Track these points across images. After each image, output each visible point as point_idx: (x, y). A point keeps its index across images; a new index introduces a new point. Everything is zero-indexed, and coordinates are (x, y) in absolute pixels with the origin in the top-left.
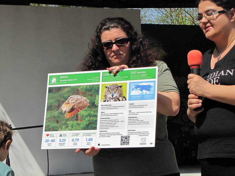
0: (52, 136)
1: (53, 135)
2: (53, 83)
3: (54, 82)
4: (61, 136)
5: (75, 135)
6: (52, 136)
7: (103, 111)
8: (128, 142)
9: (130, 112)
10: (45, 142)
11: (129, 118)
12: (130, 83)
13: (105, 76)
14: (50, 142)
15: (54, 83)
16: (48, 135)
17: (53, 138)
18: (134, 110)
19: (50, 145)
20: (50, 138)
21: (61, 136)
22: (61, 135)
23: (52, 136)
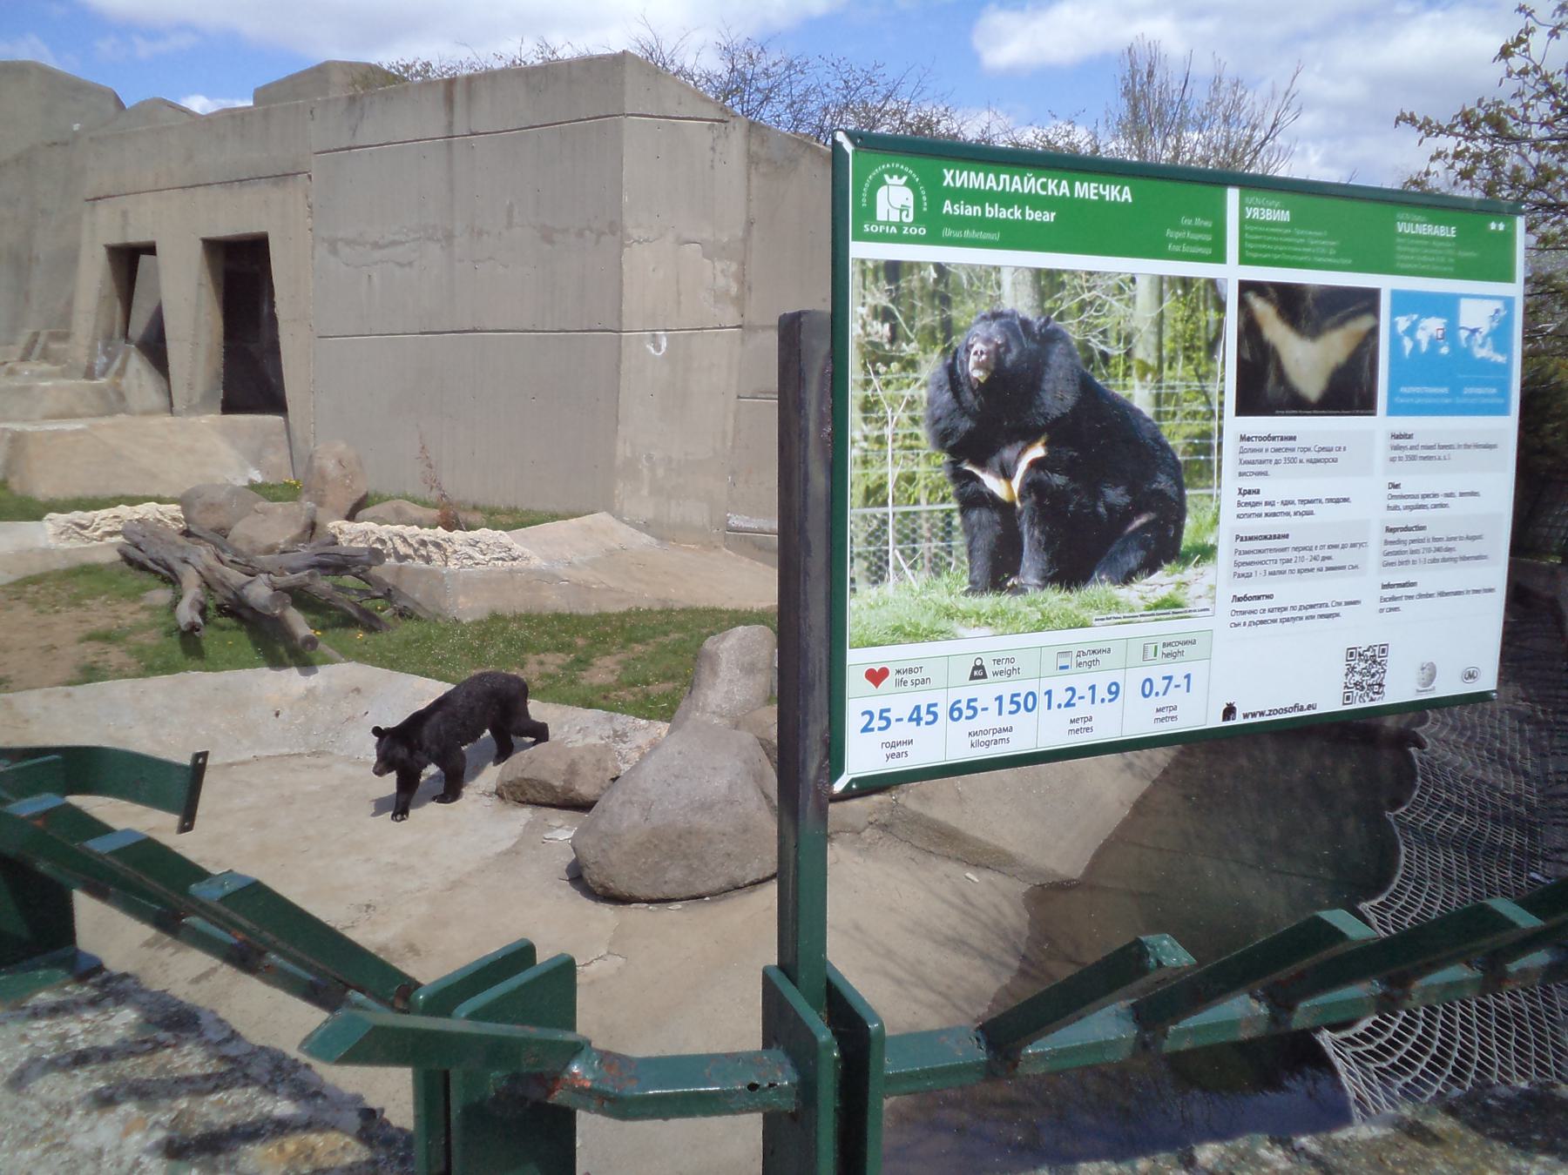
0: (906, 677)
1: (919, 676)
2: (888, 223)
3: (895, 217)
4: (978, 673)
5: (1079, 665)
6: (915, 683)
7: (1248, 484)
8: (1380, 685)
9: (1395, 492)
10: (866, 729)
11: (1391, 537)
12: (1396, 295)
13: (1253, 222)
14: (897, 732)
15: (900, 225)
16: (876, 677)
17: (923, 698)
18: (1416, 480)
19: (899, 749)
20: (900, 702)
21: (978, 673)
22: (981, 667)
23: (915, 683)
